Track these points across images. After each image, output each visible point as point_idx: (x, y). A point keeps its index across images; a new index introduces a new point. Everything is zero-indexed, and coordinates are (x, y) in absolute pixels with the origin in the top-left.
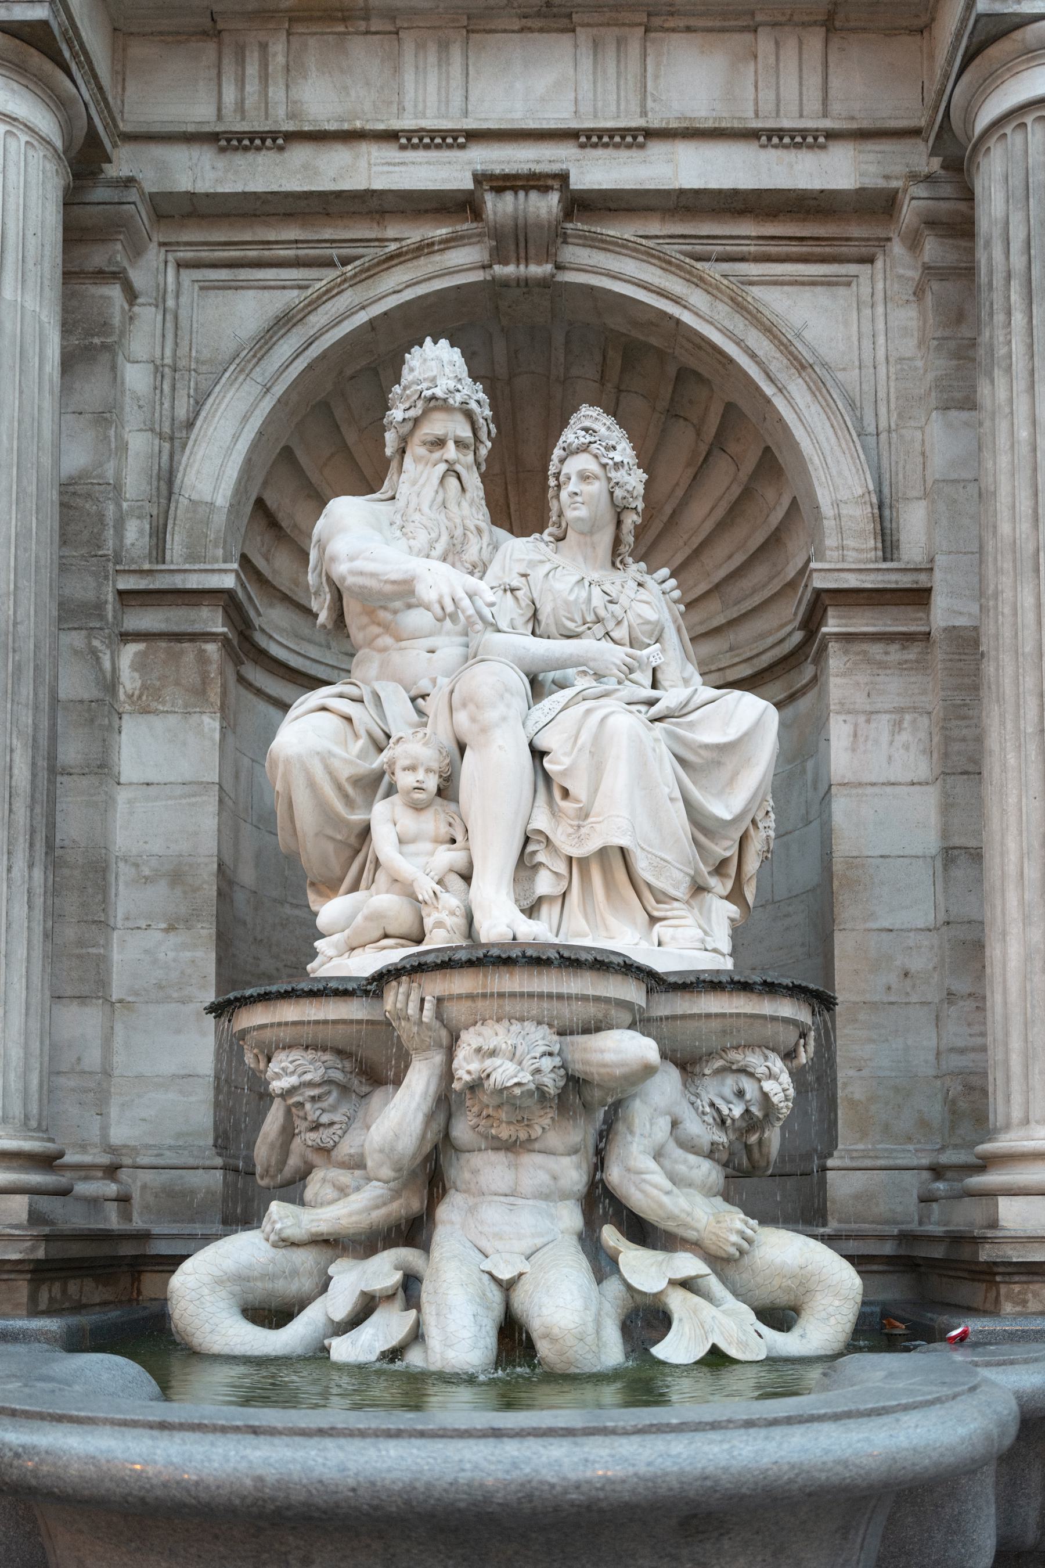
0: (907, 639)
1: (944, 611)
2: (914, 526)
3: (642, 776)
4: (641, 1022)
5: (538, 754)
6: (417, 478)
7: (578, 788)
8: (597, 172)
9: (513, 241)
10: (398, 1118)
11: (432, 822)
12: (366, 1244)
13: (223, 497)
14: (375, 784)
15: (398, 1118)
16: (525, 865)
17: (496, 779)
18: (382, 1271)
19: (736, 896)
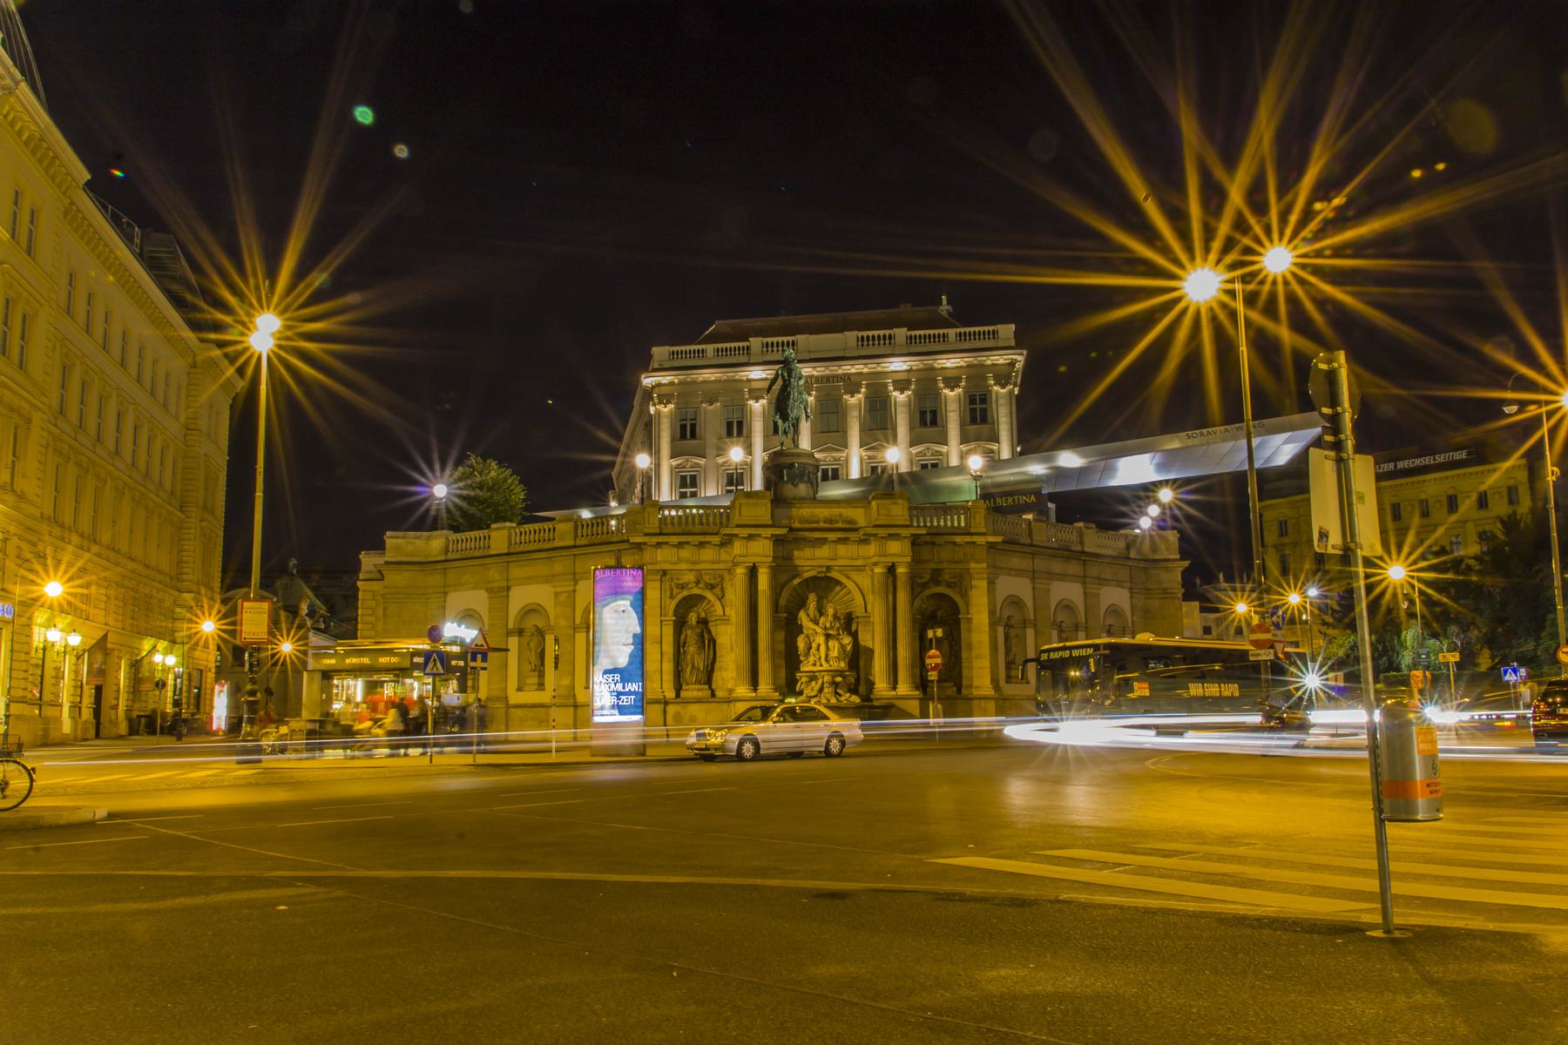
10: (816, 686)
15: (816, 686)
17: (823, 648)
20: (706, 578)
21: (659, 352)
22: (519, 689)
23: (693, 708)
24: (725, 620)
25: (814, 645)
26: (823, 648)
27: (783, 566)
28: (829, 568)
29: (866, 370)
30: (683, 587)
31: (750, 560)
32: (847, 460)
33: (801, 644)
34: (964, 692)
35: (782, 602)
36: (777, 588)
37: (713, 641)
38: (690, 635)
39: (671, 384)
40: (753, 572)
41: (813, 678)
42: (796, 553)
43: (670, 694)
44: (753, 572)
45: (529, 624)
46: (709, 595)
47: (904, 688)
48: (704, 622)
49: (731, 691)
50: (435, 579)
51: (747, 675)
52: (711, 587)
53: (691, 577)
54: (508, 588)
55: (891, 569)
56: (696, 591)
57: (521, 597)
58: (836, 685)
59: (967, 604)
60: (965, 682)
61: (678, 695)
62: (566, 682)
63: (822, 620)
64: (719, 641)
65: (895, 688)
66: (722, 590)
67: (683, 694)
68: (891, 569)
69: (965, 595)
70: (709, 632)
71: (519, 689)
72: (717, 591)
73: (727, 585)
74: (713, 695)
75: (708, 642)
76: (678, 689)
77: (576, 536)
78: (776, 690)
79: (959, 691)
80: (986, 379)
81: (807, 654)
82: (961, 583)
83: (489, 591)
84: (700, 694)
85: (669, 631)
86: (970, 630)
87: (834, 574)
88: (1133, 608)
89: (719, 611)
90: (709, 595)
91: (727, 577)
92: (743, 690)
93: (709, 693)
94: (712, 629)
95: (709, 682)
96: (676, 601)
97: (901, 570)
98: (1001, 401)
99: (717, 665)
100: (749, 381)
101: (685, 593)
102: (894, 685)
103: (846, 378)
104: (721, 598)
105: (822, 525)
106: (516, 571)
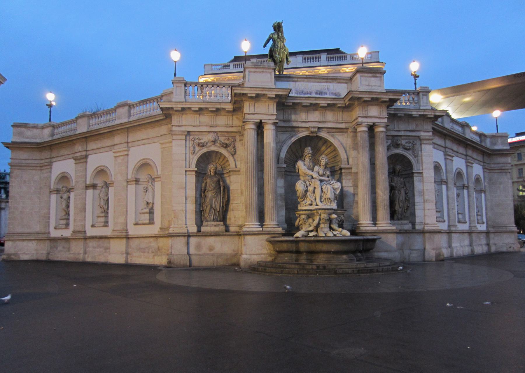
0: (350, 172)
1: (354, 170)
2: (351, 161)
3: (331, 191)
4: (334, 213)
5: (322, 189)
6: (307, 160)
7: (326, 192)
8: (321, 125)
9: (312, 132)
11: (312, 195)
12: (311, 231)
13: (284, 157)
14: (306, 191)
16: (321, 199)
17: (318, 191)
18: (314, 233)
19: (336, 200)
20: (222, 139)
22: (93, 226)
23: (211, 240)
24: (237, 171)
25: (311, 188)
26: (318, 191)
27: (283, 128)
30: (203, 145)
31: (257, 118)
33: (300, 187)
34: (418, 227)
35: (283, 155)
36: (279, 144)
37: (227, 189)
38: (210, 183)
40: (260, 127)
41: (310, 215)
42: (293, 117)
43: (193, 229)
44: (260, 127)
45: (99, 182)
46: (223, 151)
47: (384, 223)
48: (220, 175)
49: (241, 226)
50: (46, 154)
51: (255, 214)
52: (226, 146)
53: (211, 137)
54: (86, 157)
55: (371, 128)
56: (213, 148)
57: (94, 161)
58: (330, 221)
59: (418, 162)
60: (418, 220)
61: (199, 231)
62: (121, 220)
63: (316, 168)
64: (231, 188)
65: (375, 224)
66: (234, 147)
67: (203, 229)
68: (371, 128)
70: (224, 181)
71: (93, 226)
72: (231, 149)
73: (238, 144)
74: (227, 230)
75: (223, 189)
76: (199, 224)
77: (130, 116)
78: (278, 225)
79: (414, 228)
81: (305, 196)
83: (75, 159)
84: (217, 229)
85: (192, 179)
87: (323, 134)
89: (232, 165)
90: (223, 151)
91: (238, 138)
92: (253, 226)
93: (223, 228)
94: (228, 180)
95: (224, 219)
96: (199, 155)
97: (380, 129)
99: (231, 207)
101: (205, 150)
102: (374, 220)
104: (234, 154)
105: (314, 95)
106: (92, 145)
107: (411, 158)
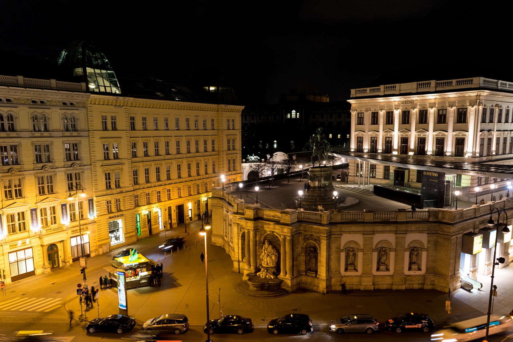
21: (353, 91)
28: (273, 232)
29: (419, 99)
32: (410, 136)
34: (318, 276)
39: (355, 103)
69: (319, 244)
79: (316, 276)
80: (466, 103)
82: (318, 240)
85: (240, 241)
86: (320, 256)
88: (429, 242)
98: (471, 113)
100: (380, 102)
103: (412, 102)
107: (317, 245)
